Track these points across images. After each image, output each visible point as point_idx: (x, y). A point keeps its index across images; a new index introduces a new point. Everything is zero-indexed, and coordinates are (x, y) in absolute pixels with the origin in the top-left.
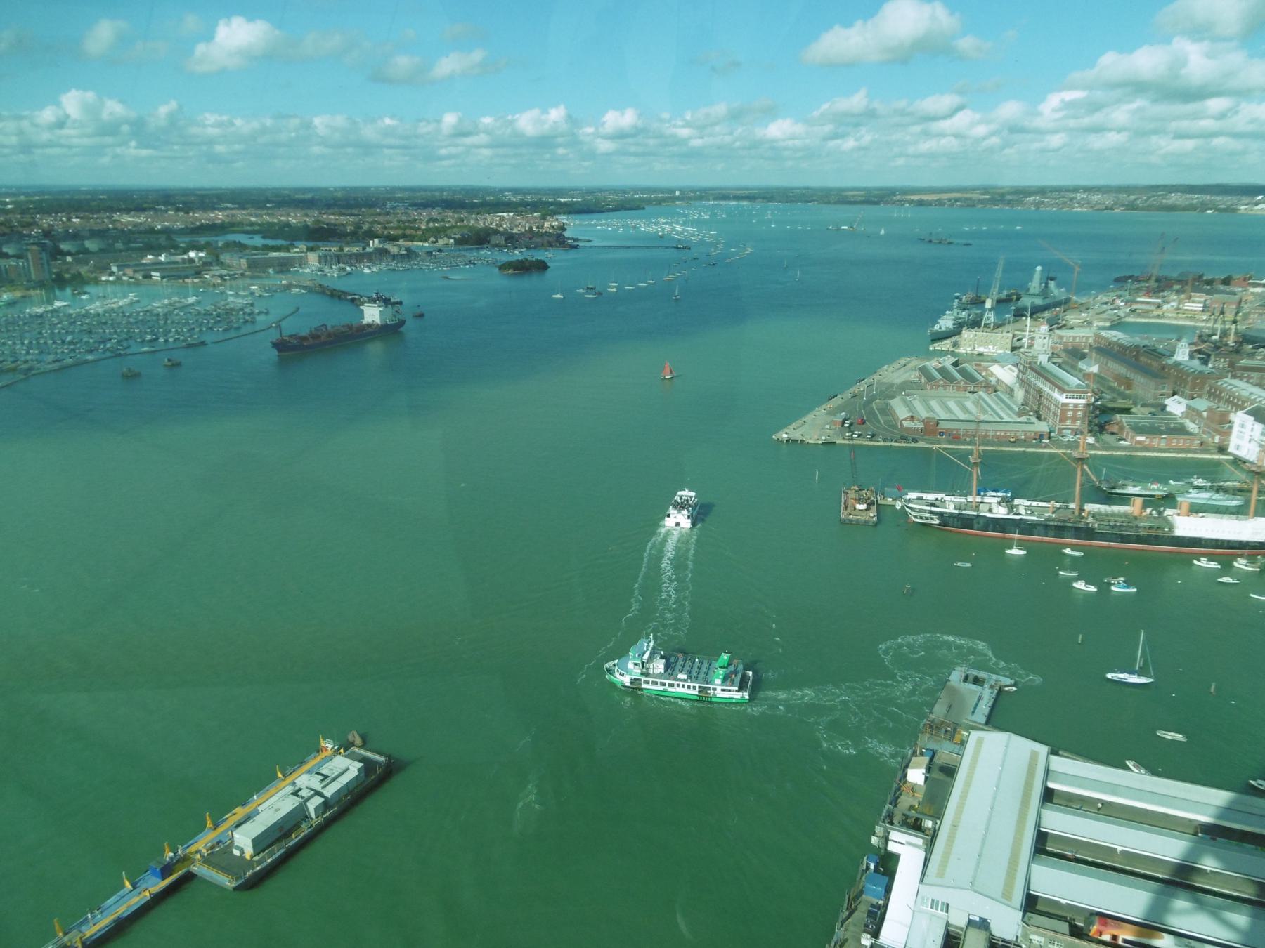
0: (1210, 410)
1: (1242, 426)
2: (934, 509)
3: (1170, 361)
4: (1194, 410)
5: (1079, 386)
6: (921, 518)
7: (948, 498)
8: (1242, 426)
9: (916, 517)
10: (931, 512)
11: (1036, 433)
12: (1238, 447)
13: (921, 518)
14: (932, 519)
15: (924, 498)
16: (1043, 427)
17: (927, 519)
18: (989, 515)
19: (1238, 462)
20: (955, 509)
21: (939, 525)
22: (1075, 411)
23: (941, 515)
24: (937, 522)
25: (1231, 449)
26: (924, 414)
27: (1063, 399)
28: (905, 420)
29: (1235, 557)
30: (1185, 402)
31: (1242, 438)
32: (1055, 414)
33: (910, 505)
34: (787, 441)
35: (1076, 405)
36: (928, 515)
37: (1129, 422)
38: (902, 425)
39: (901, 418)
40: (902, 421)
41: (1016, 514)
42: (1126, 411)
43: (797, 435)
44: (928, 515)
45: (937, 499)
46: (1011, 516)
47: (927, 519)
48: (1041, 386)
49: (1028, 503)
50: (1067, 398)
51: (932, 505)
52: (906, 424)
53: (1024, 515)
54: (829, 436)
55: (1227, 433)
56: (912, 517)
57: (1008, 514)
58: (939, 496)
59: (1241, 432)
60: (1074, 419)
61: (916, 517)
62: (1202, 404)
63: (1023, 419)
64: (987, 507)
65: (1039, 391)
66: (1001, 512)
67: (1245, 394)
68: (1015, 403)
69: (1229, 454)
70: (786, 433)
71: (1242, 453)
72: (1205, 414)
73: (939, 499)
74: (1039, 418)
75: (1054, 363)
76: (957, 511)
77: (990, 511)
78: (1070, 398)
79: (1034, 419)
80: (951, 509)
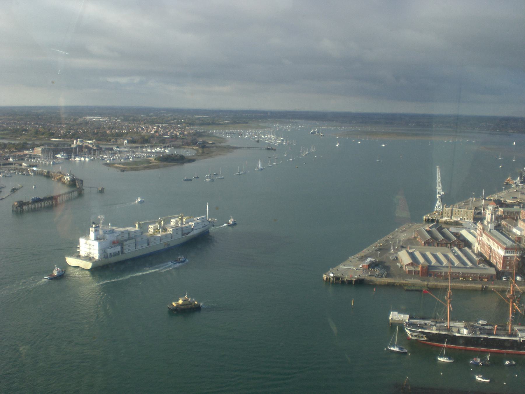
6: (416, 336)
9: (412, 335)
11: (489, 275)
13: (416, 336)
14: (422, 337)
16: (492, 271)
18: (457, 335)
20: (437, 330)
28: (408, 265)
35: (511, 257)
36: (420, 335)
44: (420, 335)
45: (426, 324)
46: (471, 335)
47: (419, 336)
51: (422, 328)
56: (410, 336)
57: (469, 334)
63: (481, 265)
64: (456, 329)
65: (490, 249)
66: (465, 332)
70: (332, 273)
73: (427, 324)
76: (437, 332)
77: (459, 332)
80: (434, 330)
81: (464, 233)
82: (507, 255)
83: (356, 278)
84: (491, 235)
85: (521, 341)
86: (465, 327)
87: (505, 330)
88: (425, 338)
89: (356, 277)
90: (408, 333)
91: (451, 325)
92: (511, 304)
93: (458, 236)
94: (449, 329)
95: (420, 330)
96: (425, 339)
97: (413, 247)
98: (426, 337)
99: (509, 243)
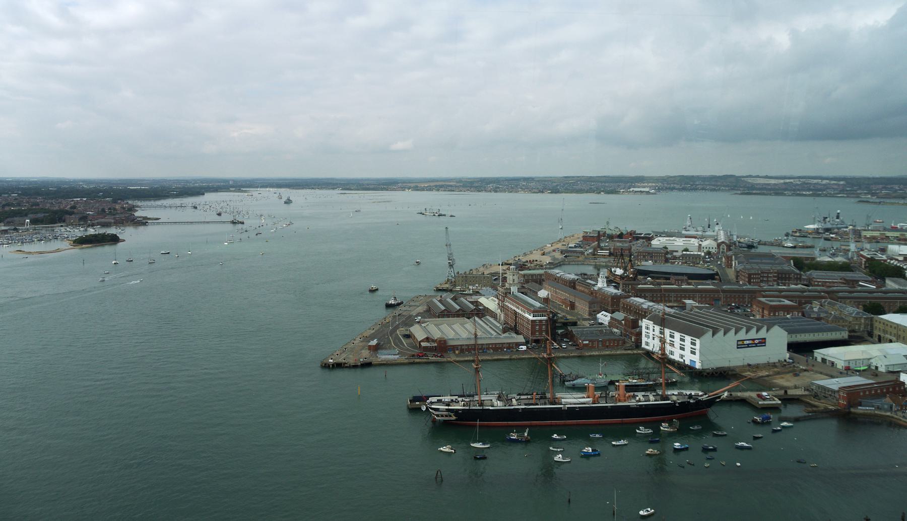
0: (625, 319)
1: (647, 328)
2: (450, 408)
3: (596, 288)
4: (616, 320)
5: (540, 308)
6: (442, 416)
7: (460, 399)
8: (647, 328)
9: (438, 416)
10: (448, 410)
12: (647, 344)
13: (442, 416)
14: (450, 416)
15: (443, 401)
16: (520, 339)
17: (446, 416)
18: (491, 408)
19: (649, 354)
21: (456, 420)
22: (540, 326)
23: (456, 412)
24: (454, 418)
25: (644, 345)
26: (436, 334)
27: (531, 318)
28: (422, 341)
29: (659, 423)
30: (609, 315)
31: (648, 337)
32: (528, 329)
33: (433, 406)
34: (333, 365)
35: (541, 321)
37: (578, 331)
38: (420, 344)
39: (419, 340)
40: (420, 342)
41: (509, 406)
42: (574, 324)
43: (340, 360)
45: (452, 400)
47: (446, 416)
48: (515, 309)
49: (518, 397)
50: (534, 316)
51: (448, 405)
52: (423, 344)
53: (515, 405)
54: (366, 359)
55: (640, 334)
57: (505, 406)
58: (454, 398)
59: (647, 333)
60: (541, 331)
61: (438, 416)
62: (620, 316)
63: (506, 335)
65: (516, 313)
66: (499, 405)
67: (645, 306)
68: (499, 322)
69: (644, 349)
71: (650, 348)
72: (623, 322)
74: (517, 333)
75: (522, 293)
78: (536, 316)
79: (514, 335)
81: (482, 300)
82: (535, 318)
83: (361, 362)
84: (516, 300)
85: (566, 409)
86: (499, 398)
87: (545, 398)
88: (454, 417)
89: (361, 360)
90: (433, 413)
91: (482, 399)
92: (549, 365)
93: (476, 303)
94: (481, 404)
95: (447, 407)
96: (454, 418)
97: (426, 320)
98: (455, 415)
99: (538, 304)
